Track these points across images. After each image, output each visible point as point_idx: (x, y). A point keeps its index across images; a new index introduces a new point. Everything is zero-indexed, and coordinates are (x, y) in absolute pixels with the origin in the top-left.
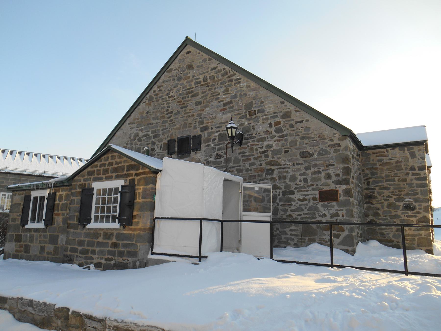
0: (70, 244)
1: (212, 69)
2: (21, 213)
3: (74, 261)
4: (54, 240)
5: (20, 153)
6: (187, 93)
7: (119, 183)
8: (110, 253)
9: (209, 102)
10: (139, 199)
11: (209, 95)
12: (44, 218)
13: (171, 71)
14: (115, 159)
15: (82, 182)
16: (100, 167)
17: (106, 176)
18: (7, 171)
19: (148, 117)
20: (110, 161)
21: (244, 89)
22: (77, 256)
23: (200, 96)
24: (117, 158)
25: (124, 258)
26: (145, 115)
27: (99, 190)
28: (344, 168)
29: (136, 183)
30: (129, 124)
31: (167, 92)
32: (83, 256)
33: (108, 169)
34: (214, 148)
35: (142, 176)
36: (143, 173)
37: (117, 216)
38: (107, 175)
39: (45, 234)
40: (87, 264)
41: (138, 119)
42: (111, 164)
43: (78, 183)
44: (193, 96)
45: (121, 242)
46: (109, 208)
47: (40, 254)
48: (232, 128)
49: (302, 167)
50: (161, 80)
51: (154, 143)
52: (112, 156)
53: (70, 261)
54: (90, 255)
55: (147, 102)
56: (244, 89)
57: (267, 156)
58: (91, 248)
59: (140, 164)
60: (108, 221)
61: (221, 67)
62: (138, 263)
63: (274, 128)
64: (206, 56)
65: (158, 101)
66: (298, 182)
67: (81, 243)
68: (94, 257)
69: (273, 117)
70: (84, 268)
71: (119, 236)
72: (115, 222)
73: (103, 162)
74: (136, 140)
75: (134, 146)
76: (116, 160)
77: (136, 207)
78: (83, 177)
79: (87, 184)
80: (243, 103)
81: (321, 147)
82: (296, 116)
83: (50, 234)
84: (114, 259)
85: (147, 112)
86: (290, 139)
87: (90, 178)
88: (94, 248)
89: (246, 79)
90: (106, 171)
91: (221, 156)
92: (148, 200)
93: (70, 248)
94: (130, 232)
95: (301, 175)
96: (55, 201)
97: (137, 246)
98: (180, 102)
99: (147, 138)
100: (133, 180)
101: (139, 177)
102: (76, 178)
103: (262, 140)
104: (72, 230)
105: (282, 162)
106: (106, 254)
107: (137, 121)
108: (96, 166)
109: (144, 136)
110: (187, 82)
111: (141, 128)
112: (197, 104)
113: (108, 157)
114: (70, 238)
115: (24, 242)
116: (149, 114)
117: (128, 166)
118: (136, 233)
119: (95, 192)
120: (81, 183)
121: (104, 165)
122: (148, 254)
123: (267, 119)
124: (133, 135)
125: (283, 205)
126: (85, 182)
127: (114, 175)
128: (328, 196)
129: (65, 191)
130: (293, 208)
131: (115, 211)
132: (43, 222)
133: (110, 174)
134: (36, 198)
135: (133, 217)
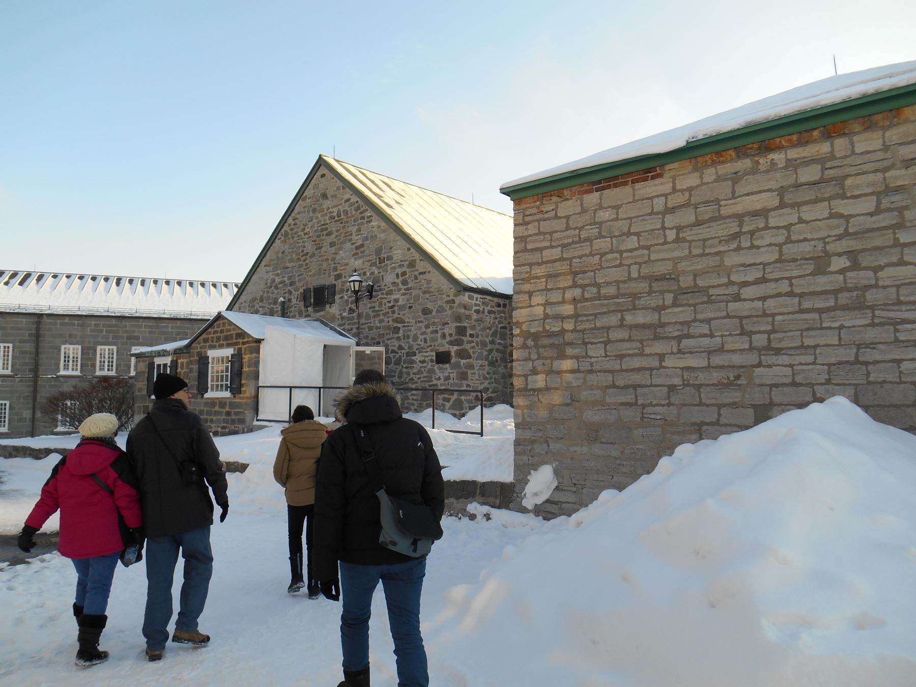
1: (346, 201)
2: (146, 382)
5: (155, 282)
6: (322, 230)
7: (228, 352)
8: (225, 421)
9: (342, 243)
11: (343, 235)
13: (305, 199)
15: (199, 350)
18: (137, 315)
21: (375, 229)
23: (334, 236)
26: (280, 255)
28: (457, 327)
31: (302, 227)
34: (347, 301)
42: (222, 331)
44: (327, 235)
46: (222, 376)
48: (354, 281)
49: (423, 325)
50: (296, 211)
51: (290, 292)
56: (375, 229)
57: (393, 312)
58: (209, 417)
60: (222, 390)
61: (354, 199)
63: (401, 279)
64: (340, 184)
65: (293, 238)
66: (419, 342)
68: (213, 425)
69: (401, 266)
71: (232, 405)
73: (216, 329)
77: (244, 376)
80: (373, 248)
81: (439, 303)
82: (422, 266)
85: (283, 252)
86: (414, 292)
89: (377, 218)
90: (218, 339)
91: (353, 311)
95: (423, 334)
98: (315, 241)
100: (240, 349)
102: (194, 345)
103: (390, 293)
105: (407, 320)
108: (210, 333)
110: (322, 216)
112: (332, 244)
118: (244, 401)
119: (210, 360)
123: (394, 268)
125: (406, 368)
127: (225, 343)
128: (442, 358)
130: (415, 371)
131: (227, 381)
134: (159, 366)
135: (241, 385)
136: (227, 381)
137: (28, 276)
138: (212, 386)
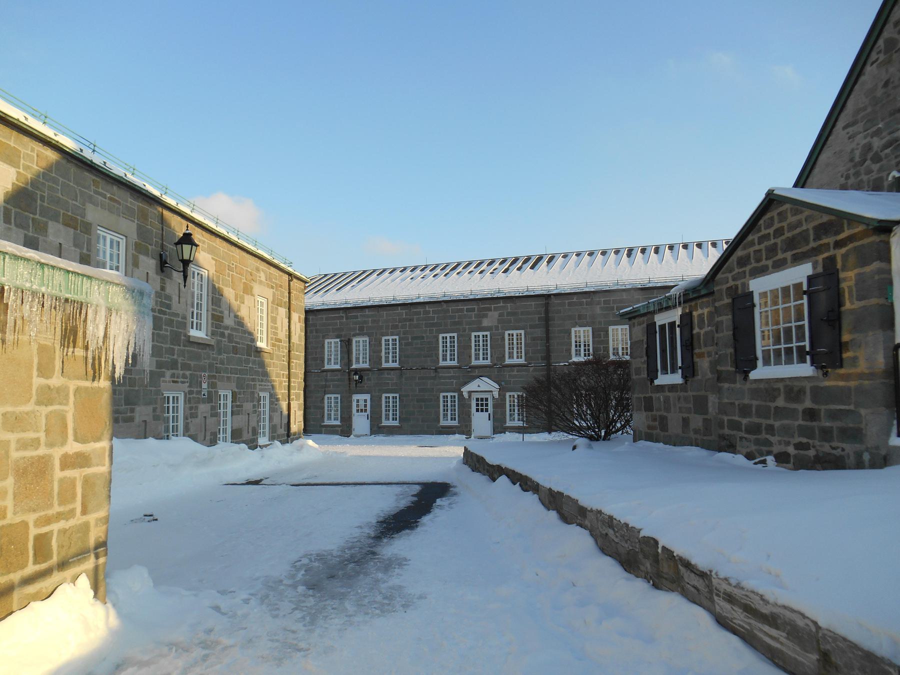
0: (726, 414)
2: (645, 358)
3: (738, 448)
4: (701, 405)
5: (671, 247)
7: (800, 273)
10: (852, 303)
12: (680, 364)
14: (786, 219)
15: (731, 283)
16: (759, 244)
17: (774, 262)
18: (651, 285)
19: (889, 95)
20: (777, 225)
22: (741, 438)
24: (789, 215)
25: (834, 444)
26: (880, 92)
27: (763, 295)
29: (839, 266)
30: (845, 128)
32: (752, 437)
33: (775, 244)
35: (850, 246)
36: (851, 239)
37: (808, 349)
38: (775, 259)
39: (685, 394)
40: (762, 455)
41: (865, 109)
42: (779, 232)
43: (724, 287)
45: (823, 407)
46: (788, 331)
47: (683, 432)
52: (779, 214)
53: (731, 448)
54: (764, 436)
55: (882, 57)
58: (764, 422)
59: (841, 219)
60: (789, 361)
62: (866, 457)
67: (745, 411)
68: (774, 439)
70: (755, 464)
71: (818, 394)
72: (804, 362)
74: (868, 162)
75: (865, 178)
76: (788, 221)
77: (846, 323)
78: (730, 272)
79: (740, 286)
83: (694, 394)
84: (814, 447)
85: (886, 84)
87: (744, 272)
88: (771, 422)
90: (772, 250)
92: (874, 301)
93: (728, 420)
94: (841, 384)
96: (692, 329)
97: (860, 416)
99: (895, 148)
100: (832, 260)
101: (843, 250)
102: (720, 276)
104: (726, 385)
106: (796, 435)
107: (862, 114)
108: (752, 244)
109: (888, 145)
111: (874, 129)
113: (772, 218)
114: (726, 401)
115: (657, 410)
116: (891, 86)
117: (816, 228)
118: (852, 384)
120: (728, 285)
121: (766, 237)
122: (888, 435)
124: (857, 153)
126: (736, 283)
127: (788, 255)
129: (707, 307)
131: (801, 338)
132: (680, 371)
133: (780, 256)
134: (662, 327)
135: (842, 346)
136: (801, 338)
137: (540, 258)
138: (766, 354)
